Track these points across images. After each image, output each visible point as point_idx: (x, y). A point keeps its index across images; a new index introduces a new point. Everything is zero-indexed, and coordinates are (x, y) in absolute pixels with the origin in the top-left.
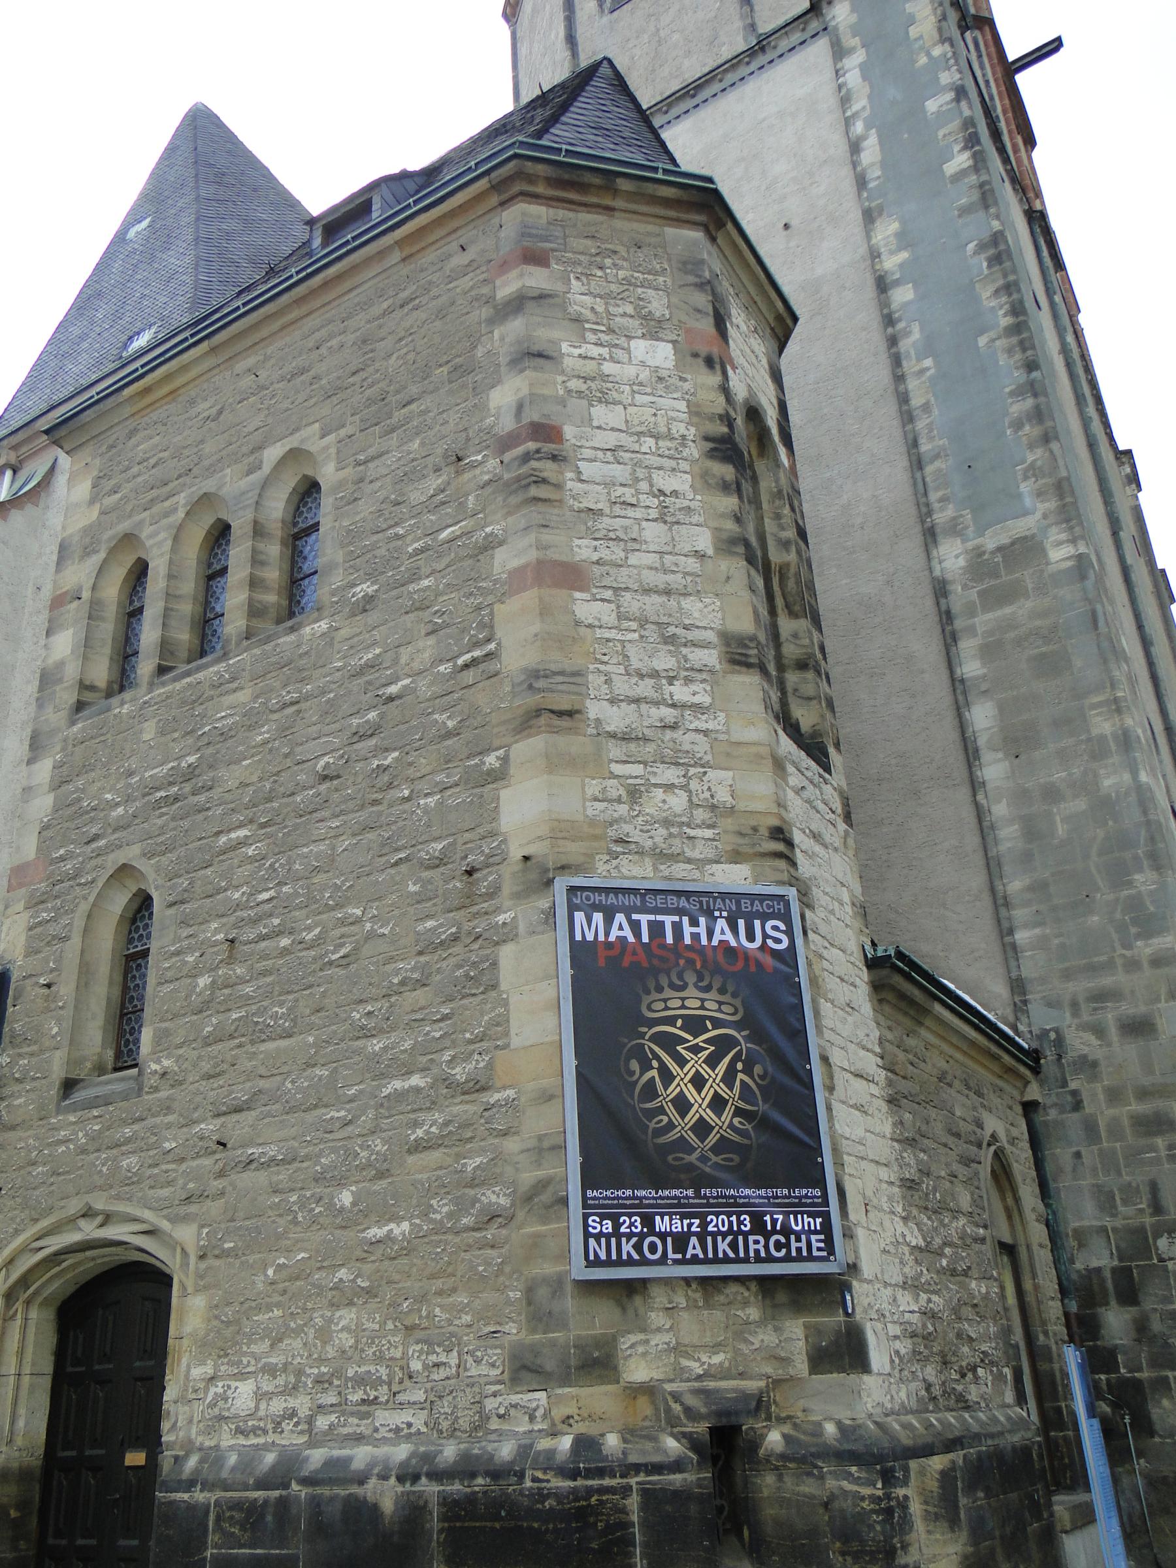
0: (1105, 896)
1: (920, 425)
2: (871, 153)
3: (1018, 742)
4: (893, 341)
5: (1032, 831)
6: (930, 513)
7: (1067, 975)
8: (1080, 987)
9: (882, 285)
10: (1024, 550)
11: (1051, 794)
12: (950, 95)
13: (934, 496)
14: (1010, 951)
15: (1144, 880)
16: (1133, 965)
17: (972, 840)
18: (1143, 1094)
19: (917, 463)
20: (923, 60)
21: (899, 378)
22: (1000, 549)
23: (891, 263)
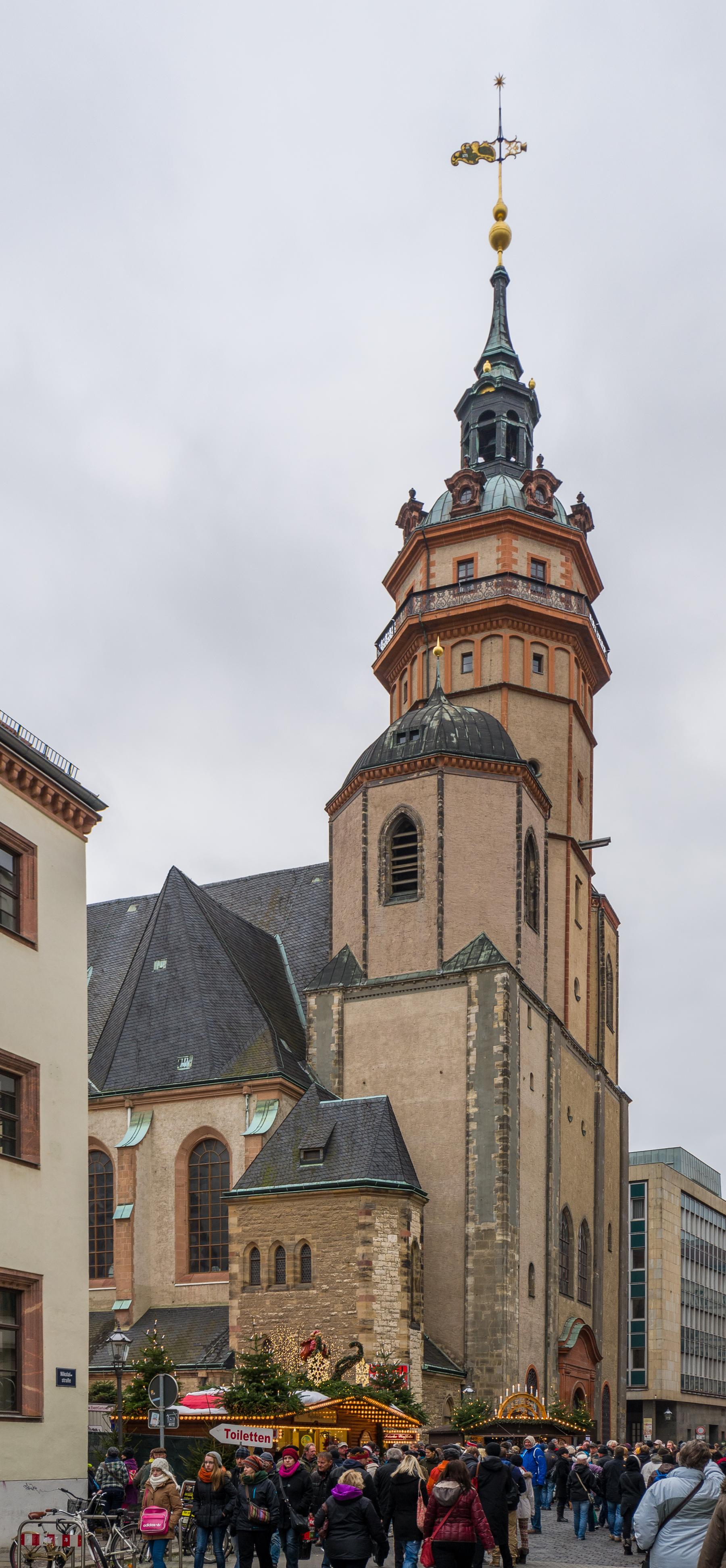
0: (489, 1337)
1: (470, 1179)
2: (473, 1059)
3: (478, 1291)
4: (468, 1143)
5: (477, 1316)
6: (468, 1211)
7: (477, 1355)
8: (480, 1358)
9: (468, 1119)
10: (490, 1233)
11: (483, 1308)
12: (501, 1048)
13: (470, 1206)
14: (466, 1346)
15: (499, 1335)
16: (492, 1355)
17: (462, 1314)
18: (488, 1386)
19: (467, 1192)
20: (496, 1026)
21: (467, 1158)
22: (484, 1230)
23: (473, 1110)
